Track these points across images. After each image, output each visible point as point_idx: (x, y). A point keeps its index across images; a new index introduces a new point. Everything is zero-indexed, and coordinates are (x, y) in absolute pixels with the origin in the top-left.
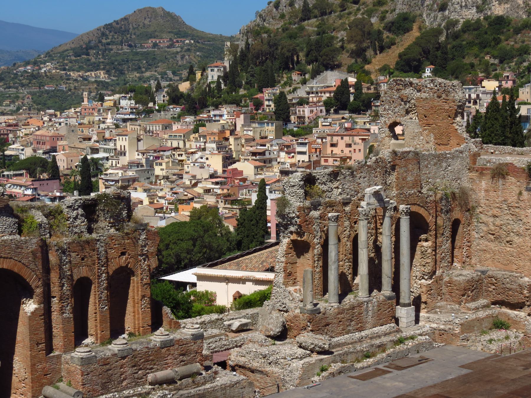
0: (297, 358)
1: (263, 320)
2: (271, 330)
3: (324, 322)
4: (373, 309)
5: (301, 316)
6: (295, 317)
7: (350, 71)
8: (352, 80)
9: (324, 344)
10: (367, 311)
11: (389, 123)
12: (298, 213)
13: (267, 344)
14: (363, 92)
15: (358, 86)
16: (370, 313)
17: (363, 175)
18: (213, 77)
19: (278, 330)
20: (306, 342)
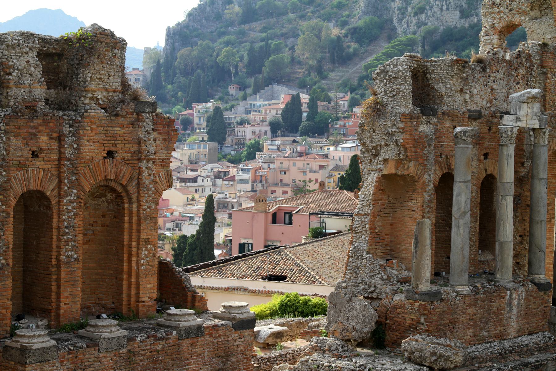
1: (336, 313)
2: (355, 329)
4: (518, 304)
5: (408, 306)
6: (395, 307)
7: (303, 86)
8: (305, 98)
9: (457, 354)
10: (510, 304)
11: (498, 26)
12: (401, 125)
13: (347, 354)
14: (319, 111)
15: (312, 105)
16: (515, 311)
17: (499, 76)
19: (366, 330)
20: (421, 351)
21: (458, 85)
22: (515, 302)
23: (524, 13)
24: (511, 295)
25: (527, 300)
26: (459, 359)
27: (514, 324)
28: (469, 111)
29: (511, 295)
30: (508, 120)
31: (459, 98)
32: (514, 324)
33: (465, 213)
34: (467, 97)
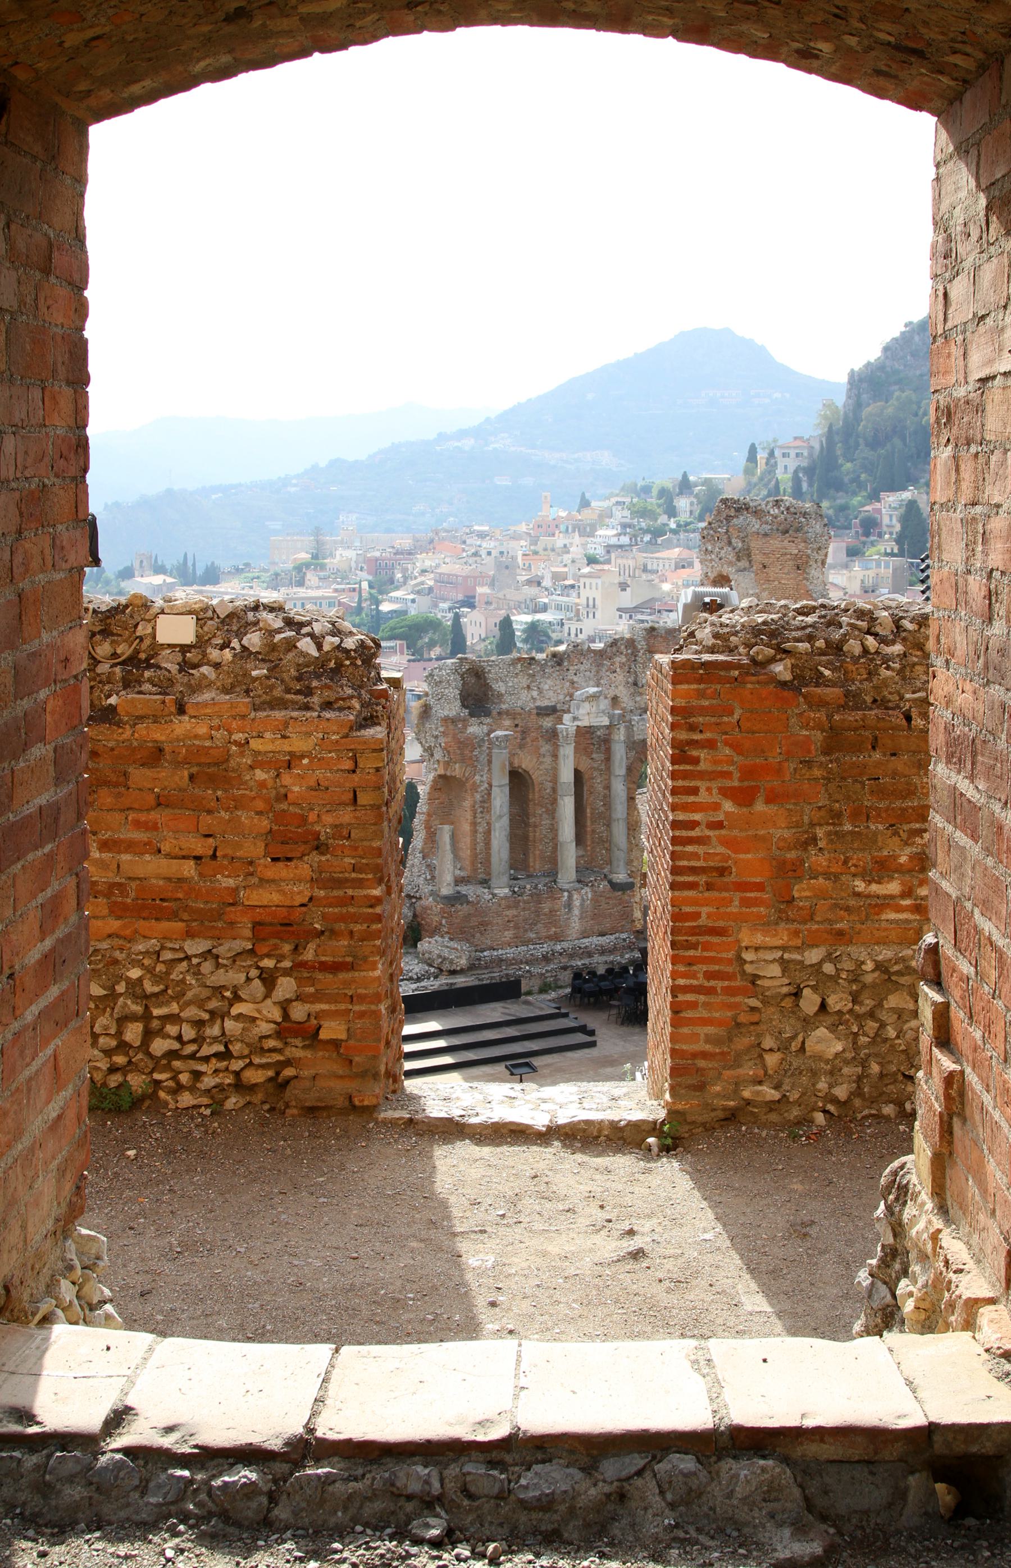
0: (411, 979)
3: (474, 921)
4: (582, 905)
10: (569, 905)
16: (576, 912)
17: (582, 668)
18: (786, 467)
21: (524, 681)
22: (577, 903)
23: (730, 564)
24: (570, 897)
25: (595, 900)
26: (463, 962)
27: (575, 925)
28: (537, 708)
29: (570, 897)
30: (567, 718)
31: (524, 695)
32: (575, 925)
33: (500, 817)
34: (535, 694)
